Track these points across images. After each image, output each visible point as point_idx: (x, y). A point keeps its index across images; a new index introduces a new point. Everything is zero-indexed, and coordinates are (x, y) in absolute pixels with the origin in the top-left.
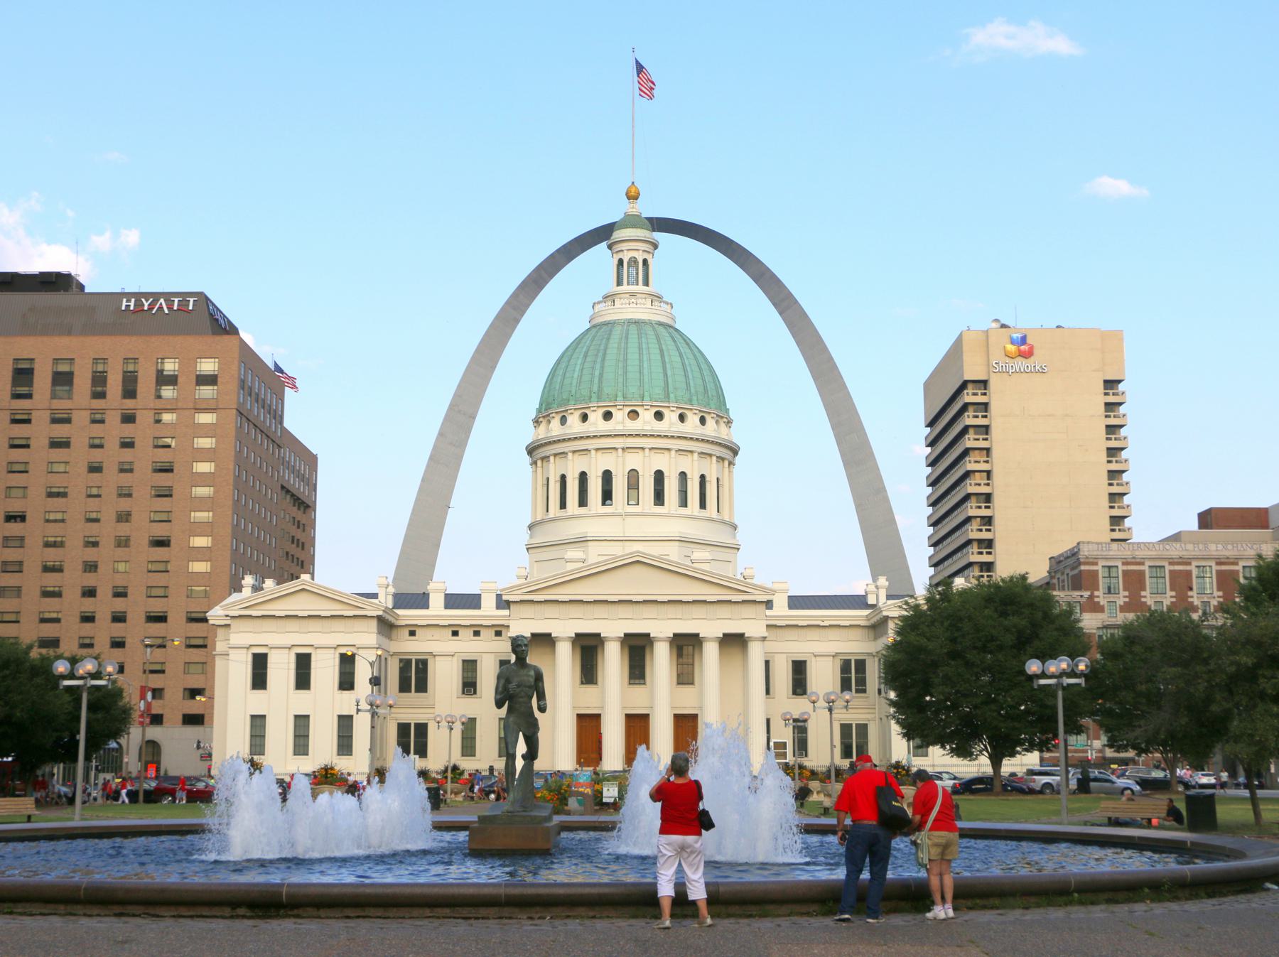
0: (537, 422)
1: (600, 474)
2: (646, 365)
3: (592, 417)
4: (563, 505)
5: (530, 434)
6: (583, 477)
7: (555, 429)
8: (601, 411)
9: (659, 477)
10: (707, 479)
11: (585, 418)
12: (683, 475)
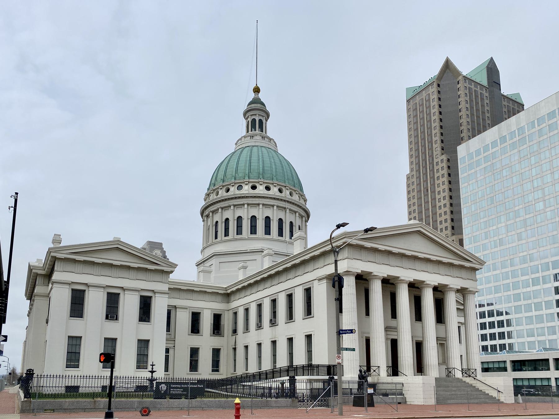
1: (236, 218)
3: (232, 189)
4: (216, 238)
7: (213, 197)
10: (294, 224)
11: (228, 190)
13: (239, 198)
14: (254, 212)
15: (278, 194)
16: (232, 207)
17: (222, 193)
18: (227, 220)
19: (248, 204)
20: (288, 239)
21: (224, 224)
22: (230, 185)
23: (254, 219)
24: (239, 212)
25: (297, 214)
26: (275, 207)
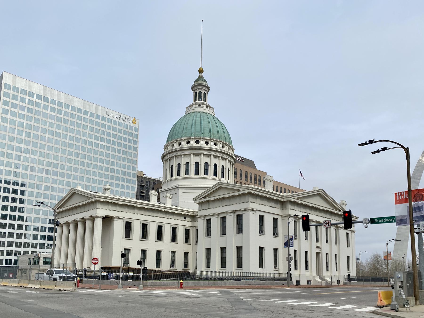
0: (165, 149)
1: (185, 164)
2: (202, 124)
4: (172, 176)
6: (179, 165)
7: (169, 148)
9: (206, 164)
10: (225, 167)
11: (180, 144)
12: (215, 166)
13: (188, 149)
15: (214, 147)
16: (183, 156)
19: (194, 154)
20: (221, 178)
21: (177, 167)
22: (181, 140)
25: (227, 161)
26: (212, 156)
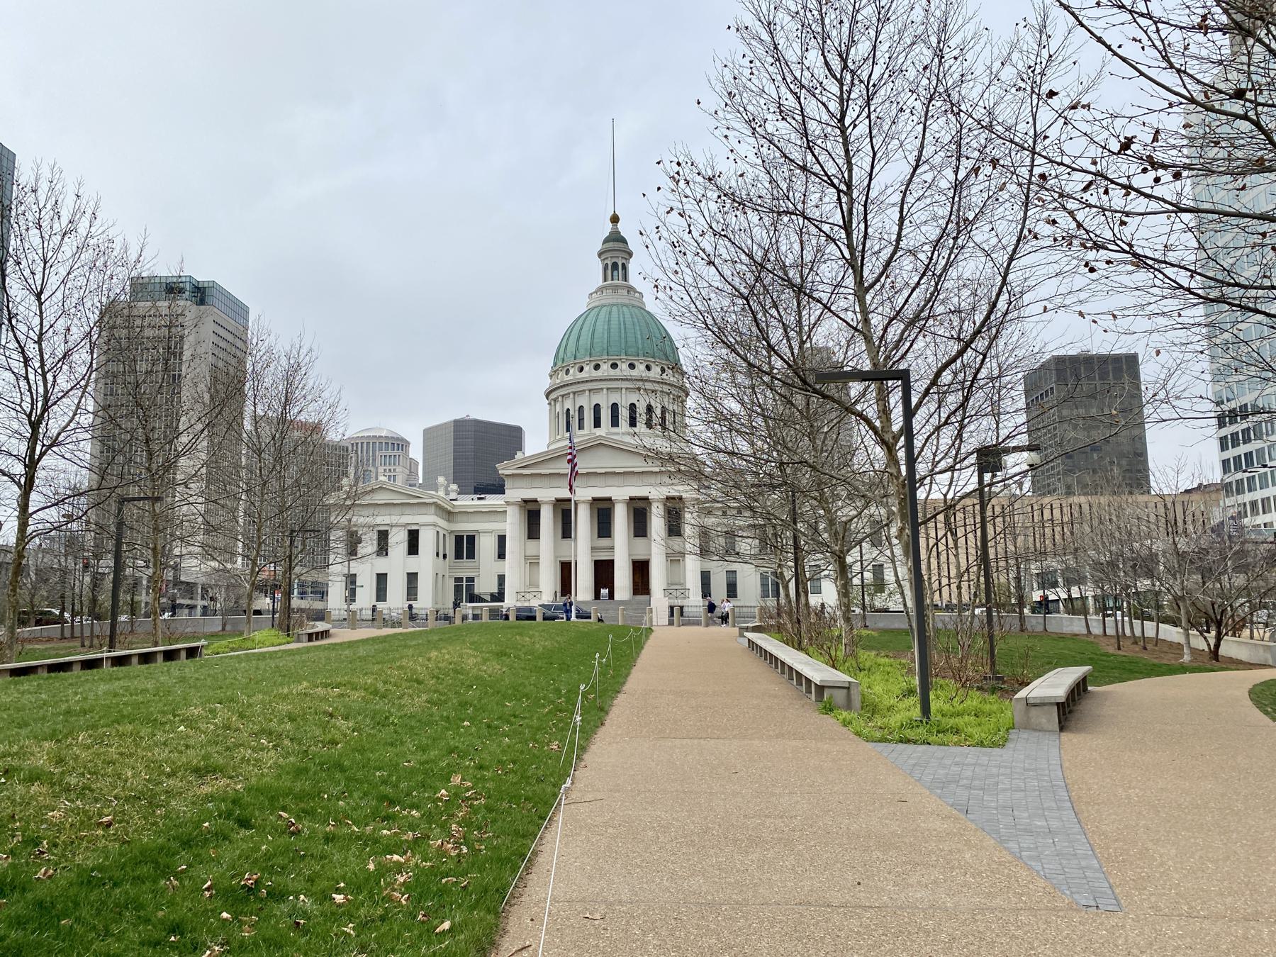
0: (551, 376)
3: (586, 368)
5: (547, 383)
7: (562, 378)
8: (593, 364)
11: (581, 369)
14: (615, 398)
17: (574, 374)
18: (581, 407)
23: (615, 407)
24: (596, 399)
